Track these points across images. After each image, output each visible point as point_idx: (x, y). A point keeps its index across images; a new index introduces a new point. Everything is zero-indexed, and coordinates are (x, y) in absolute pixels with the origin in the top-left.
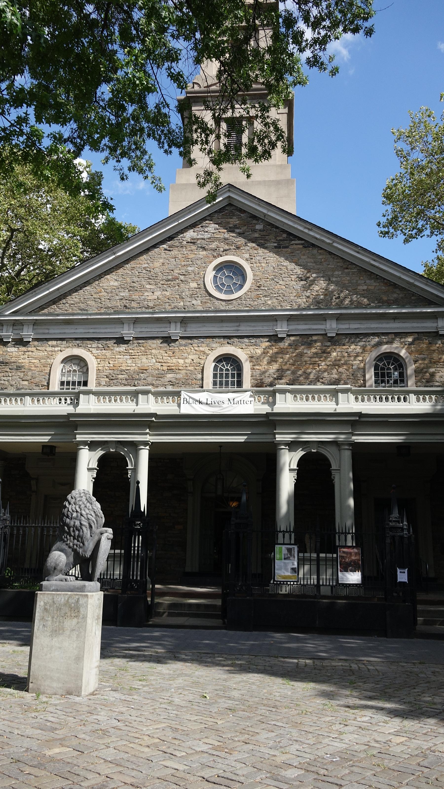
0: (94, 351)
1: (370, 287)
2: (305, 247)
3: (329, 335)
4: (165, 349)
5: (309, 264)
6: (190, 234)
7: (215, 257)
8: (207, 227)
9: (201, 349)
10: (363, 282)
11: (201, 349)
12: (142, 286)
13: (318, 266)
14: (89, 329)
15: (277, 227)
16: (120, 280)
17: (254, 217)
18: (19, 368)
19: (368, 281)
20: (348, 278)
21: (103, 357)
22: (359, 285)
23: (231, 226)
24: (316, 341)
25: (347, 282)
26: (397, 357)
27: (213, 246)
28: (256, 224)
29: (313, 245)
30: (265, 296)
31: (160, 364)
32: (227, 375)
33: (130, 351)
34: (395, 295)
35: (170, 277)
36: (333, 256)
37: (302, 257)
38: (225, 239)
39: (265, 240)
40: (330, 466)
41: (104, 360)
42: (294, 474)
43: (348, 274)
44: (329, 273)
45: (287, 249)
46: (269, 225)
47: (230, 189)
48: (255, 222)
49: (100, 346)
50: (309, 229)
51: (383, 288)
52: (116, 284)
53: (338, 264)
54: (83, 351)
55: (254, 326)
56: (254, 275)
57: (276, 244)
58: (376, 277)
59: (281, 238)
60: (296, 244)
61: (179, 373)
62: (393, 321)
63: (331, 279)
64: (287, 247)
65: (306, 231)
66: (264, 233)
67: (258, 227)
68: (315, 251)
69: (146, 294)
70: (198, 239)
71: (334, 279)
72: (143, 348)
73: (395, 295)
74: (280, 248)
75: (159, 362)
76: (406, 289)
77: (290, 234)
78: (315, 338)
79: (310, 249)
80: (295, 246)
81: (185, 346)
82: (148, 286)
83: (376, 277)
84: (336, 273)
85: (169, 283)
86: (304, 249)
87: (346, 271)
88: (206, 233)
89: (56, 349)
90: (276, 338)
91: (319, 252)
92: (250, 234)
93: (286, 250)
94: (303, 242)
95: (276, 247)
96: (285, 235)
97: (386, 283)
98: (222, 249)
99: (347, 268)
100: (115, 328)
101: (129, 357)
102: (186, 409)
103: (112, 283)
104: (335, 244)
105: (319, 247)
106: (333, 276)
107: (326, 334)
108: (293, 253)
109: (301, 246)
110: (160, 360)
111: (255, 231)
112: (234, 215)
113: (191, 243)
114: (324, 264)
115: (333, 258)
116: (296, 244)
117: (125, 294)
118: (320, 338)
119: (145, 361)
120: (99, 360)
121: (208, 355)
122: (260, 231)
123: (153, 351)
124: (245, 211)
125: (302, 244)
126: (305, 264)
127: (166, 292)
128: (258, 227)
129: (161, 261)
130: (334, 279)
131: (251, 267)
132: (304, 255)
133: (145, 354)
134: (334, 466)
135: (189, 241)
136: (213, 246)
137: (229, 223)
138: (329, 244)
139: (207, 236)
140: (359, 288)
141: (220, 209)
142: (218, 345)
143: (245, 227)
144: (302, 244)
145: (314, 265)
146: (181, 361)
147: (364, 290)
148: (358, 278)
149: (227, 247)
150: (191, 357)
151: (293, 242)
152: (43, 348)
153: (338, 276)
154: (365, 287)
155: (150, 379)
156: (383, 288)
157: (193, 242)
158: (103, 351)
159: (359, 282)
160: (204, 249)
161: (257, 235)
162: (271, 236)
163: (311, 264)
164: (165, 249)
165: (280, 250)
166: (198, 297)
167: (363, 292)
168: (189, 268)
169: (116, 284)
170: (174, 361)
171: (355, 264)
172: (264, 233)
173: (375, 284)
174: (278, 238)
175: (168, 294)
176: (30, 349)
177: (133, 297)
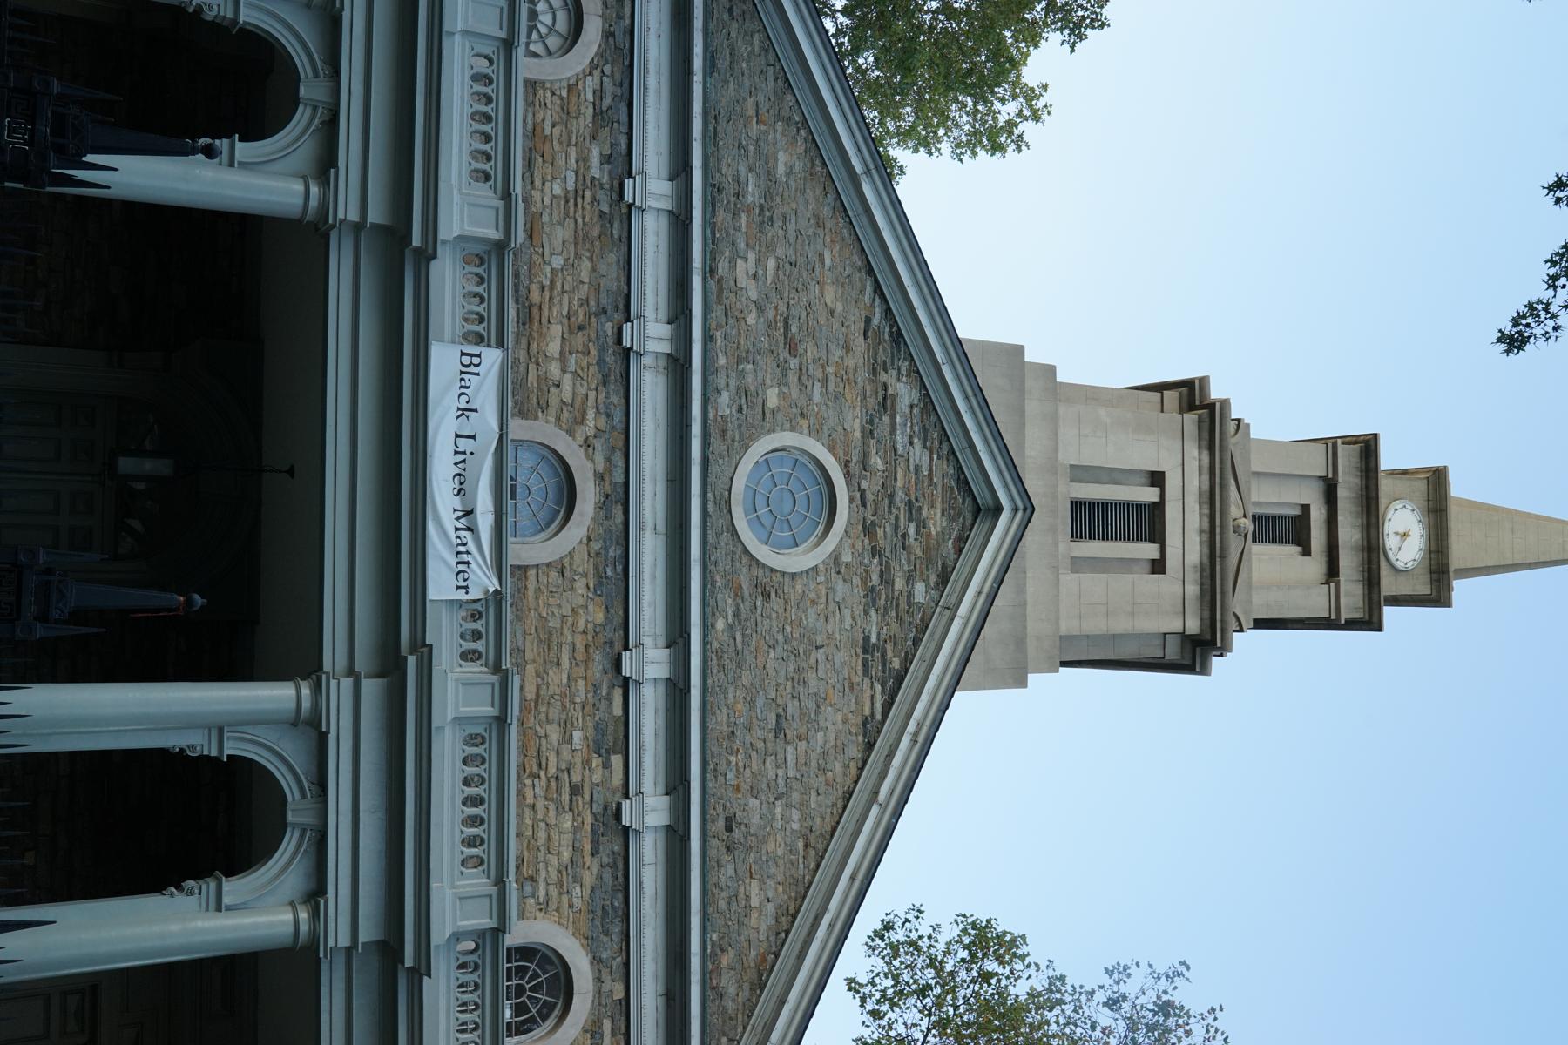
0: (591, 83)
1: (755, 914)
2: (865, 724)
3: (626, 805)
4: (592, 303)
5: (820, 735)
6: (905, 394)
7: (846, 465)
8: (925, 447)
9: (591, 414)
10: (770, 895)
11: (591, 414)
12: (771, 247)
13: (814, 764)
14: (659, 73)
15: (916, 642)
16: (792, 183)
17: (944, 578)
19: (771, 907)
20: (780, 852)
21: (573, 108)
22: (762, 882)
23: (925, 512)
24: (607, 765)
25: (771, 847)
26: (557, 1012)
28: (926, 581)
29: (870, 746)
30: (737, 614)
31: (547, 283)
33: (588, 194)
34: (732, 990)
35: (794, 330)
36: (840, 804)
37: (839, 716)
38: (891, 497)
39: (885, 609)
40: (232, 871)
42: (200, 743)
43: (792, 850)
44: (795, 796)
45: (860, 672)
46: (922, 619)
47: (1020, 514)
48: (933, 578)
49: (607, 102)
50: (916, 734)
51: (753, 953)
53: (818, 820)
54: (595, 48)
55: (654, 577)
56: (793, 575)
57: (874, 639)
58: (781, 934)
59: (890, 654)
60: (873, 697)
61: (517, 342)
62: (661, 990)
63: (778, 803)
64: (866, 672)
65: (911, 727)
66: (903, 605)
67: (919, 587)
68: (854, 752)
69: (752, 256)
70: (893, 418)
71: (778, 810)
72: (595, 233)
73: (732, 990)
74: (865, 651)
75: (552, 282)
76: (750, 1017)
77: (900, 680)
78: (616, 760)
79: (860, 738)
80: (868, 693)
81: (601, 362)
82: (771, 263)
83: (781, 934)
84: (796, 815)
85: (781, 325)
86: (859, 720)
87: (801, 844)
88: (906, 440)
90: (618, 645)
91: (853, 764)
92: (901, 565)
93: (860, 667)
94: (879, 717)
95: (867, 639)
96: (896, 664)
97: (764, 960)
98: (865, 484)
99: (806, 846)
100: (658, 154)
101: (571, 185)
102: (444, 360)
103: (782, 157)
104: (875, 810)
105: (865, 762)
106: (788, 806)
107: (627, 796)
108: (852, 688)
109: (867, 712)
110: (559, 284)
111: (910, 579)
112: (951, 520)
113: (885, 399)
114: (822, 779)
115: (834, 804)
116: (873, 697)
117: (753, 194)
118: (617, 780)
119: (558, 236)
120: (565, 94)
121: (571, 432)
122: (910, 594)
123: (586, 265)
124: (961, 551)
125: (872, 714)
126: (822, 724)
127: (754, 314)
128: (919, 587)
129: (839, 307)
130: (778, 810)
131: (815, 568)
132: (845, 721)
134: (234, 888)
135: (890, 391)
136: (877, 462)
137: (932, 506)
138: (877, 793)
139: (901, 440)
140: (755, 883)
141: (967, 483)
142: (600, 468)
143: (919, 553)
144: (872, 714)
145: (819, 750)
146: (554, 348)
147: (748, 897)
148: (780, 878)
149: (870, 497)
150: (567, 381)
151: (878, 688)
153: (786, 820)
154: (755, 902)
156: (753, 953)
157: (887, 403)
158: (590, 111)
159: (769, 882)
160: (868, 434)
161: (899, 584)
162: (894, 625)
163: (820, 742)
164: (868, 321)
165: (859, 651)
166: (740, 410)
167: (741, 896)
168: (817, 385)
169: (781, 169)
170: (556, 330)
171: (818, 866)
172: (903, 605)
173: (763, 928)
174: (889, 647)
177: (744, 216)
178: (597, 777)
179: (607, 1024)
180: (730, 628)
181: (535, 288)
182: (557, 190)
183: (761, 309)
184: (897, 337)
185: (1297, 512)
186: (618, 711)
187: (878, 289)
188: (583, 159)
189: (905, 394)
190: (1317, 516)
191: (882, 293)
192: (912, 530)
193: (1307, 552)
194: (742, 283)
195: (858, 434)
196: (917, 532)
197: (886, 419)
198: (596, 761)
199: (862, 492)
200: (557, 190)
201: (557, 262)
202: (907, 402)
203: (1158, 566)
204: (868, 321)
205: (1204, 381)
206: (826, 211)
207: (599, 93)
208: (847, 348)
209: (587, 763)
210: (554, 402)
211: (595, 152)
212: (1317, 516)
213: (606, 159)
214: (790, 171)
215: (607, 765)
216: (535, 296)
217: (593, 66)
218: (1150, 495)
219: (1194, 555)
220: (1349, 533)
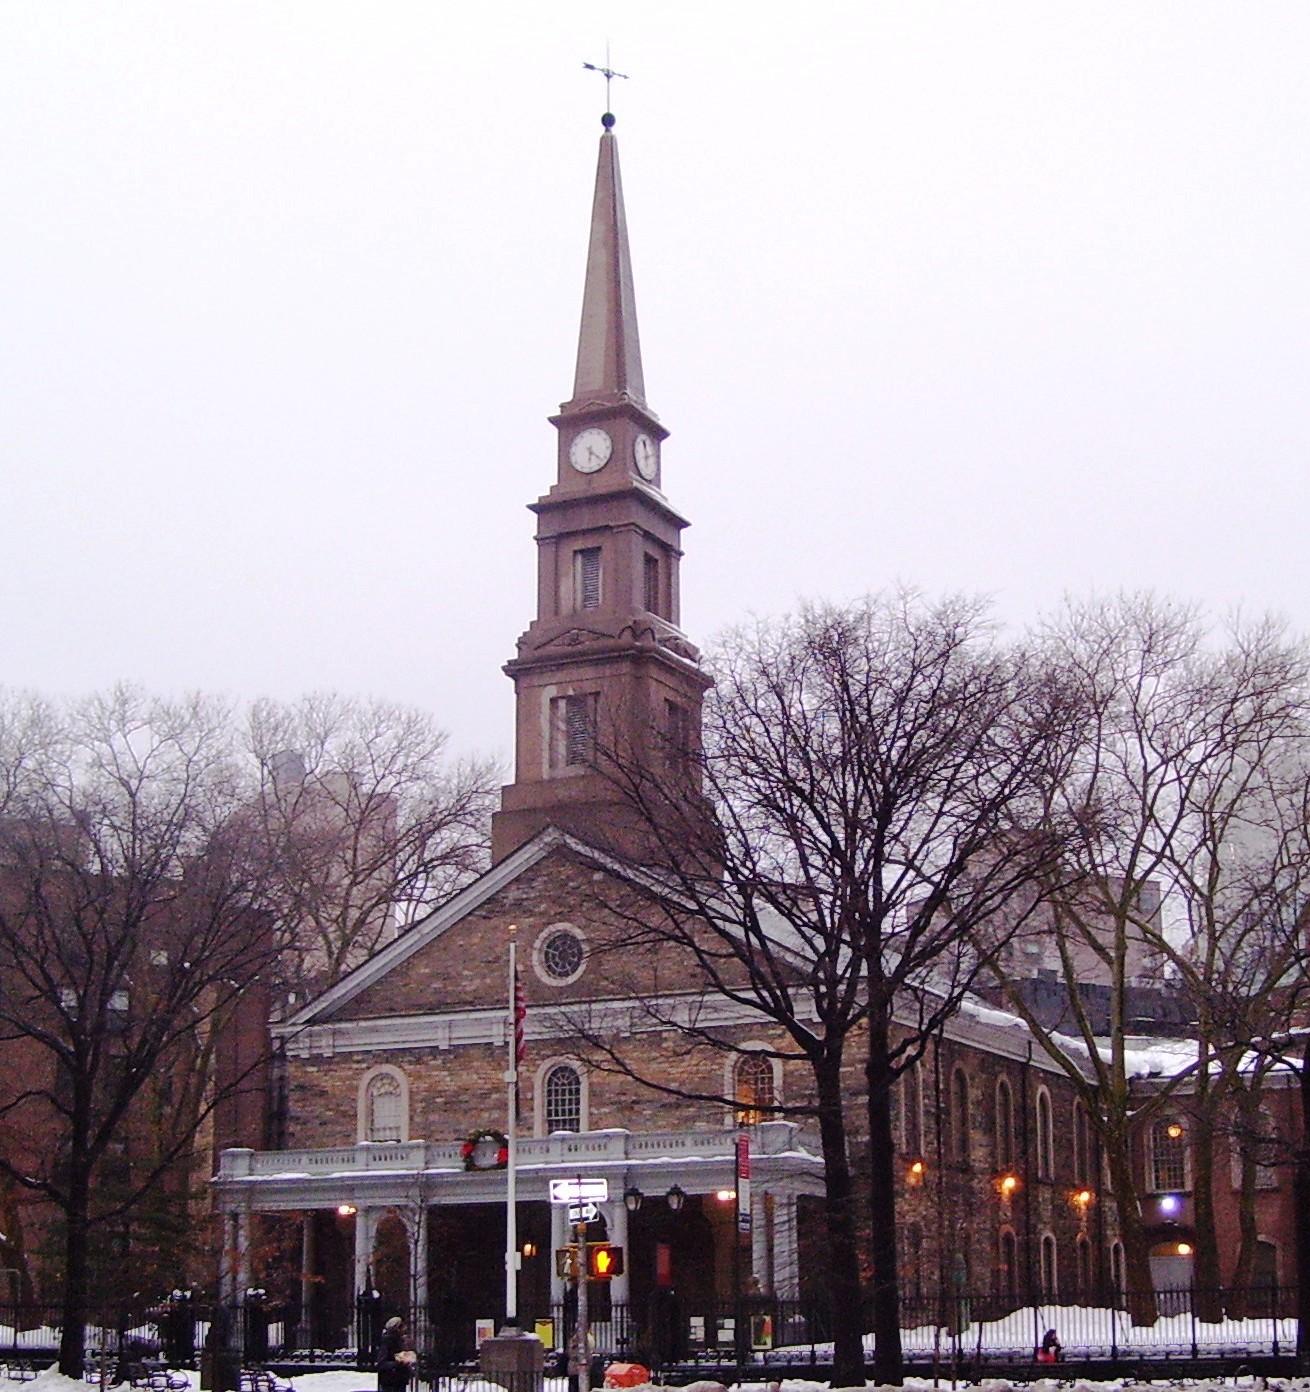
0: (407, 1067)
12: (459, 974)
18: (323, 1093)
27: (543, 907)
32: (564, 1091)
41: (420, 1077)
52: (427, 971)
70: (523, 900)
82: (466, 973)
89: (364, 1065)
98: (552, 913)
101: (446, 1073)
103: (422, 971)
117: (437, 985)
133: (466, 1067)
136: (543, 907)
152: (347, 1066)
155: (472, 1104)
157: (518, 903)
160: (531, 914)
164: (485, 918)
169: (427, 971)
175: (488, 981)
176: (332, 1067)
178: (671, 1044)
179: (771, 1032)
180: (613, 983)
181: (486, 1086)
182: (448, 1079)
183: (484, 977)
184: (489, 900)
185: (579, 558)
186: (645, 1036)
187: (470, 914)
188: (436, 1068)
189: (513, 894)
190: (579, 545)
191: (474, 910)
192: (571, 884)
193: (599, 548)
194: (473, 987)
195: (531, 919)
196: (573, 881)
197: (525, 903)
198: (664, 1045)
199: (556, 914)
200: (448, 1079)
201: (475, 1077)
202: (516, 893)
203: (597, 694)
204: (485, 918)
205: (504, 668)
206: (441, 945)
207: (410, 1063)
208: (496, 928)
209: (666, 1049)
210: (528, 1074)
211: (432, 1062)
212: (579, 545)
213: (435, 1058)
214: (426, 966)
215: (666, 1039)
216: (488, 1086)
217: (400, 1067)
218: (562, 704)
219: (588, 672)
220: (586, 519)
